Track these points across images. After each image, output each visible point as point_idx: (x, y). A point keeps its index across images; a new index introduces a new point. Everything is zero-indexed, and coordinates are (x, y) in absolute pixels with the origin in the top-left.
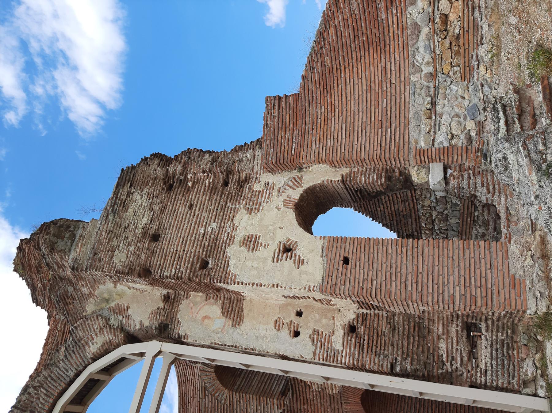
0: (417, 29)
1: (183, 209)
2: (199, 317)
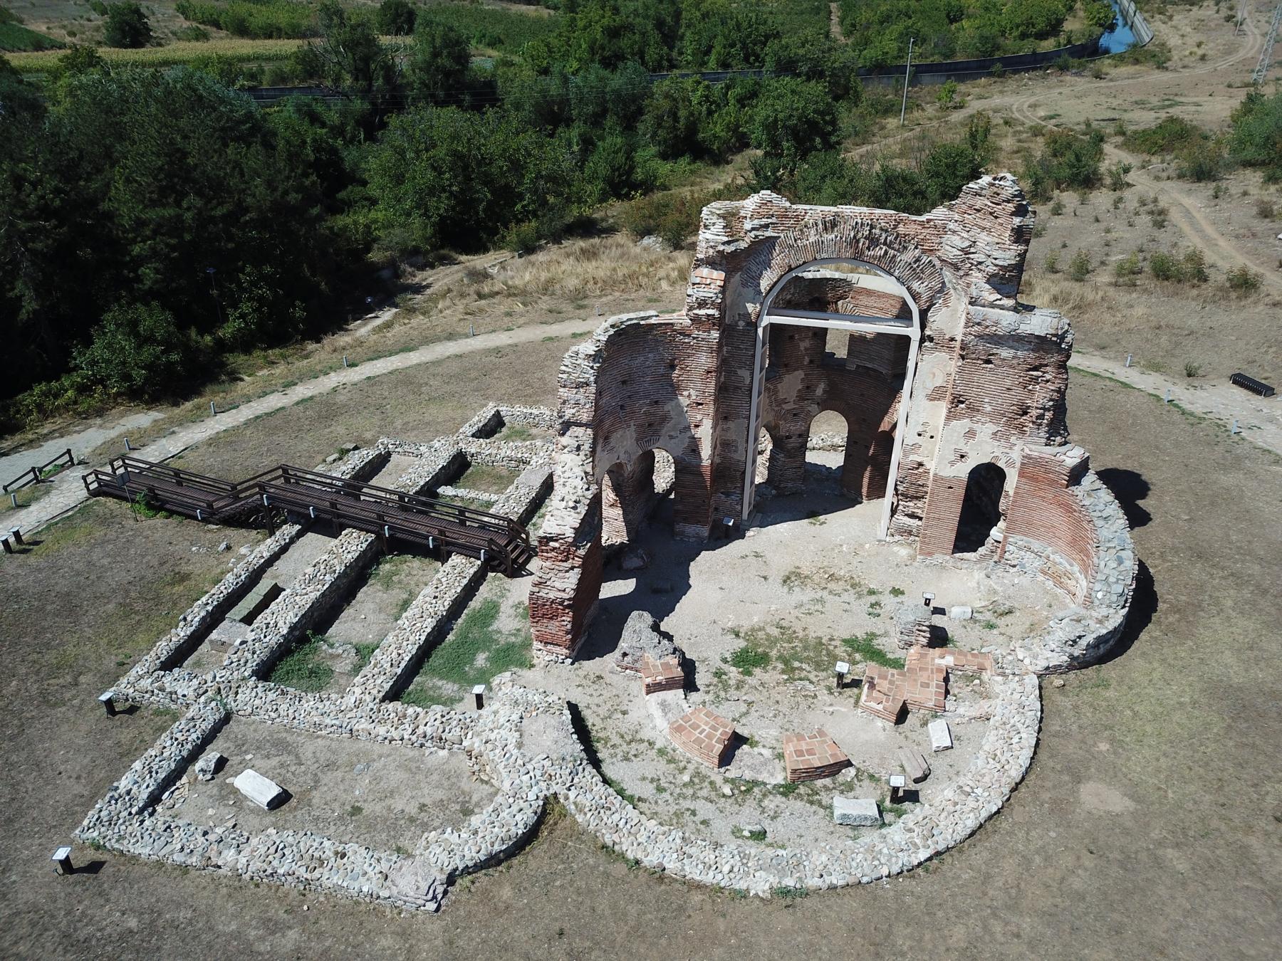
0: (1071, 565)
1: (1008, 383)
2: (935, 370)
